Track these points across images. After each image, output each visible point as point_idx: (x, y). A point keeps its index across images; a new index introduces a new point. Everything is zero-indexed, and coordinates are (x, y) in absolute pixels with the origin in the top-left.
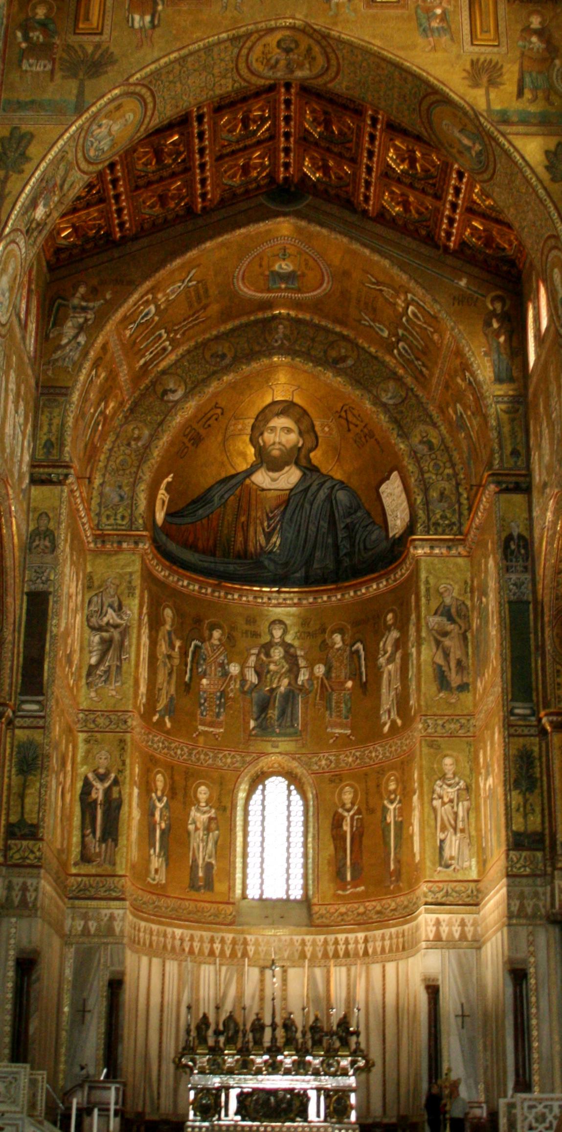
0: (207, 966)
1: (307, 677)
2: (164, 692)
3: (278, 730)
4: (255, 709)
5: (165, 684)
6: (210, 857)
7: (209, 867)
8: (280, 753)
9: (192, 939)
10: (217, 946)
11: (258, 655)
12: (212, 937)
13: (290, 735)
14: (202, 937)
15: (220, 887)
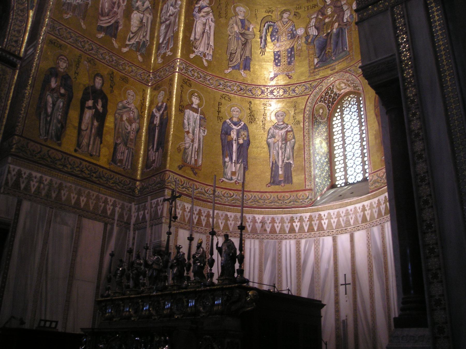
0: (288, 241)
1: (349, 15)
2: (238, 55)
3: (334, 58)
4: (317, 51)
5: (239, 50)
6: (288, 159)
7: (288, 166)
8: (337, 72)
9: (273, 221)
10: (297, 225)
11: (316, 18)
12: (292, 218)
13: (342, 57)
14: (282, 218)
15: (297, 179)
